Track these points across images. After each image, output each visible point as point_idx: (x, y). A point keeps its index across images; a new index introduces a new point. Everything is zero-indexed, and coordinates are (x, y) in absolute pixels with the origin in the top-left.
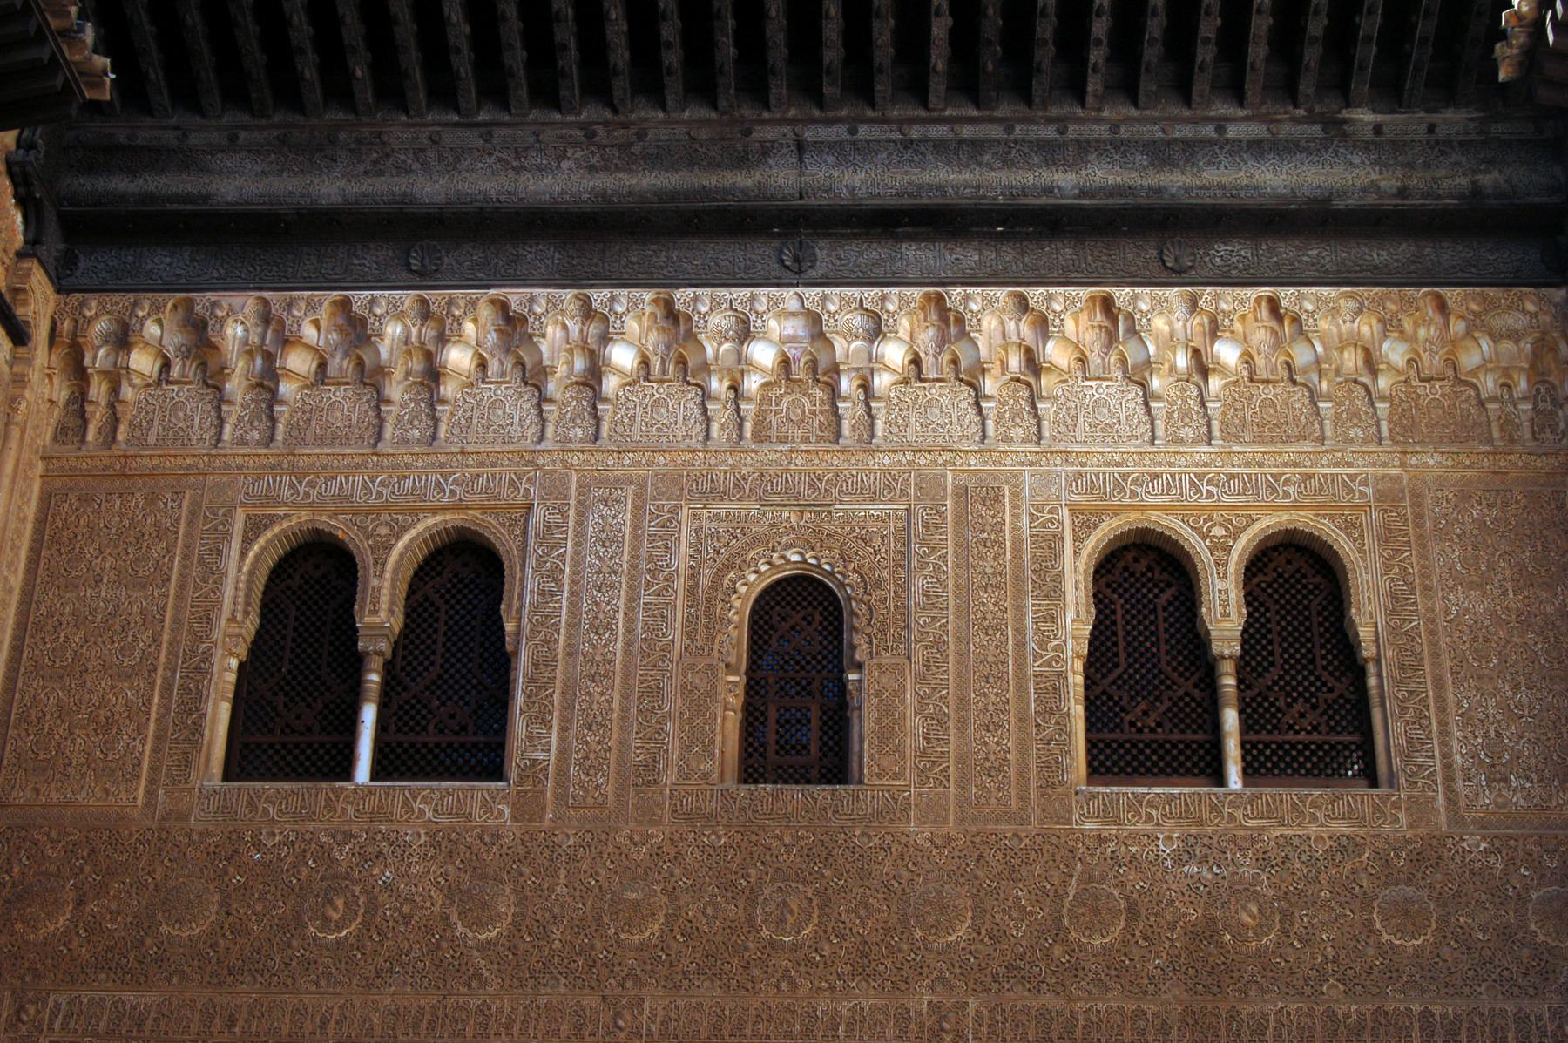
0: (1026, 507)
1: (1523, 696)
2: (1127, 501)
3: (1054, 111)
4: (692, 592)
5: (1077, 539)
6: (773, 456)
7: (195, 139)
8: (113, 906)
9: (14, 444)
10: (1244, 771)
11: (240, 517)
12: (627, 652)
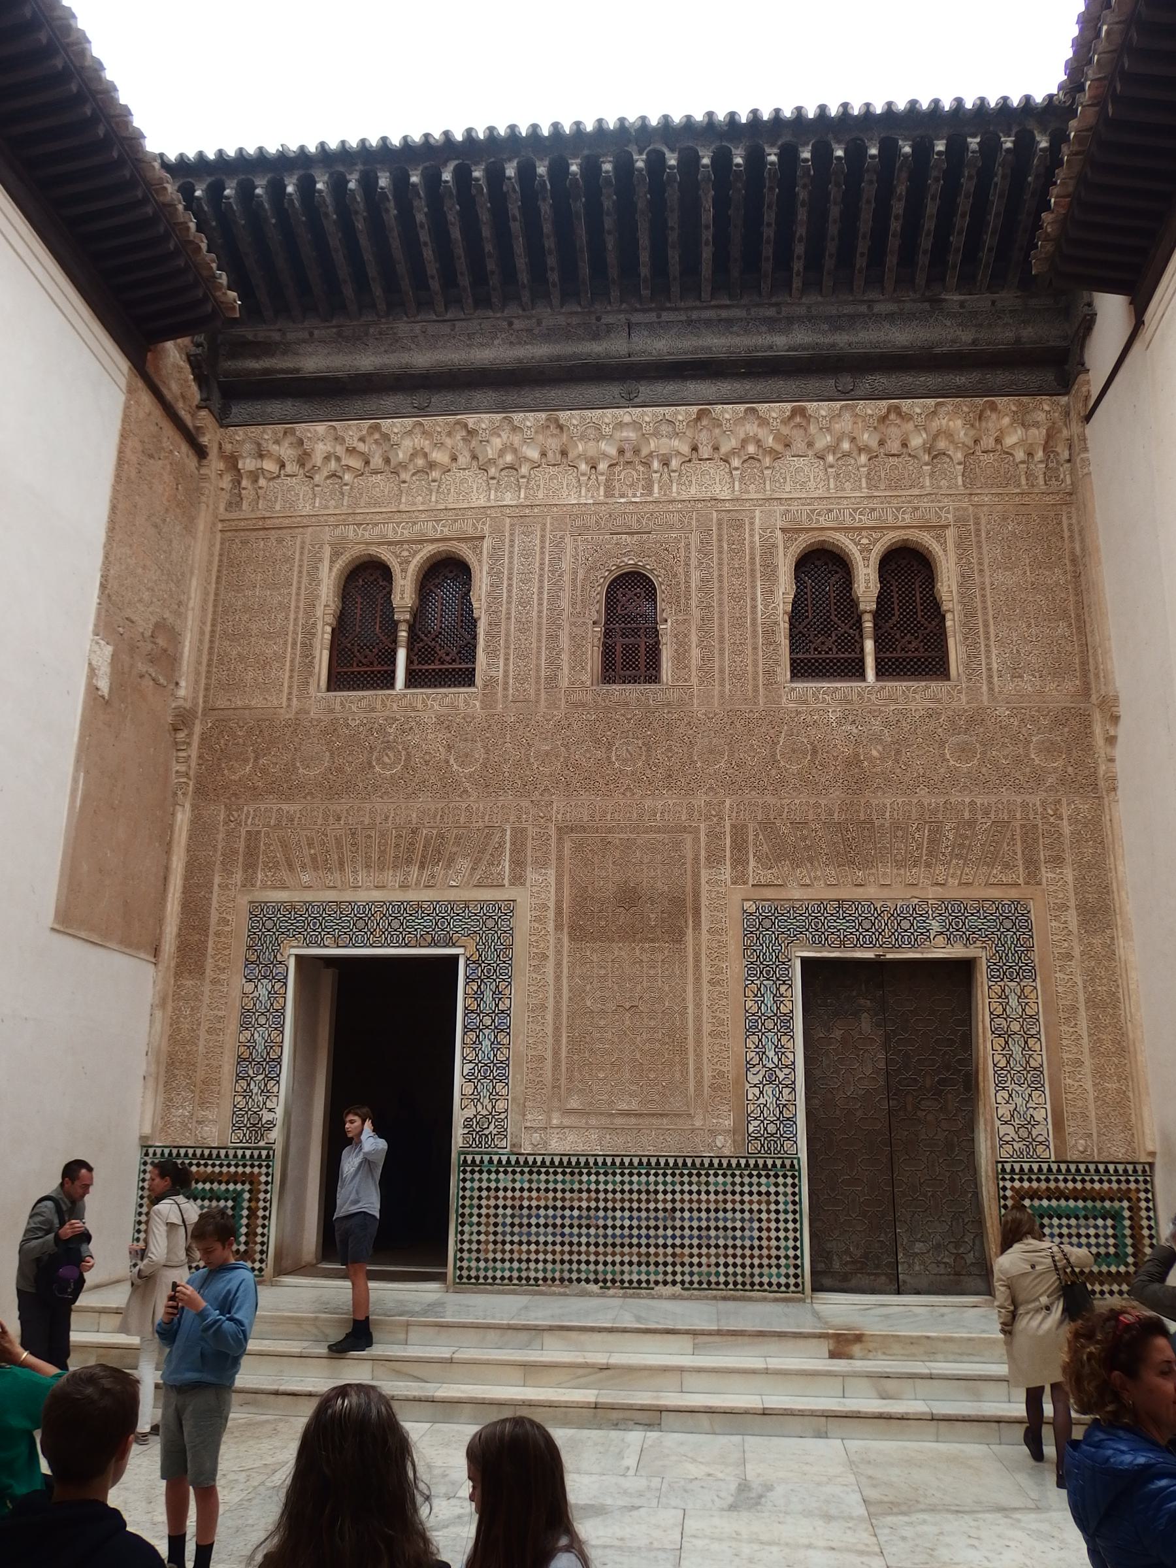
1: (1033, 631)
3: (774, 300)
4: (574, 580)
7: (291, 336)
9: (203, 514)
10: (877, 674)
12: (540, 617)
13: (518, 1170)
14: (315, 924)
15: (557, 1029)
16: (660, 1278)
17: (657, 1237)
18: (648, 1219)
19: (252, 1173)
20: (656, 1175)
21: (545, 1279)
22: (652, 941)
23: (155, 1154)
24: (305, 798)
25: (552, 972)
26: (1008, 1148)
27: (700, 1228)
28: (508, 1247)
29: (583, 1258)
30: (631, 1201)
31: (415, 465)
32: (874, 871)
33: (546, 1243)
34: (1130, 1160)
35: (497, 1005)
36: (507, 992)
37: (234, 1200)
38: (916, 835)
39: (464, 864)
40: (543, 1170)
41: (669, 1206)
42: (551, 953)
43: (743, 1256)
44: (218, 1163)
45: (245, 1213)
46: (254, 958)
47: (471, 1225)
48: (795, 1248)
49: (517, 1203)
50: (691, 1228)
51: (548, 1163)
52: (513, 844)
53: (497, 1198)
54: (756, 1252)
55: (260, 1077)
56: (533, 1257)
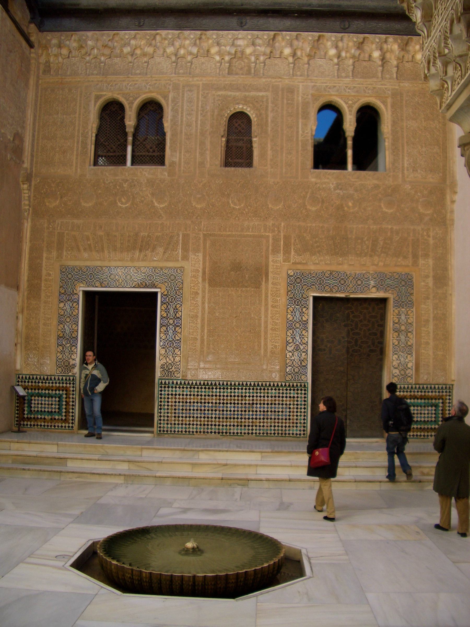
0: (300, 94)
1: (424, 149)
2: (327, 93)
5: (314, 103)
6: (234, 79)
8: (70, 198)
11: (94, 94)
13: (185, 386)
14: (91, 276)
15: (203, 326)
16: (246, 431)
17: (245, 415)
18: (242, 407)
19: (66, 387)
20: (246, 389)
21: (197, 432)
22: (246, 287)
23: (22, 378)
24: (85, 217)
25: (201, 301)
26: (396, 378)
27: (264, 411)
28: (181, 419)
29: (213, 423)
30: (234, 400)
31: (136, 54)
32: (347, 258)
33: (197, 417)
34: (445, 383)
35: (176, 315)
36: (180, 309)
37: (59, 398)
38: (367, 242)
39: (160, 250)
40: (196, 387)
41: (251, 402)
42: (200, 292)
43: (282, 423)
44: (51, 382)
45: (64, 403)
46: (63, 291)
47: (164, 409)
48: (304, 419)
49: (185, 401)
50: (260, 411)
51: (198, 384)
52: (183, 240)
53: (176, 398)
54: (288, 421)
55: (68, 345)
56: (191, 423)
